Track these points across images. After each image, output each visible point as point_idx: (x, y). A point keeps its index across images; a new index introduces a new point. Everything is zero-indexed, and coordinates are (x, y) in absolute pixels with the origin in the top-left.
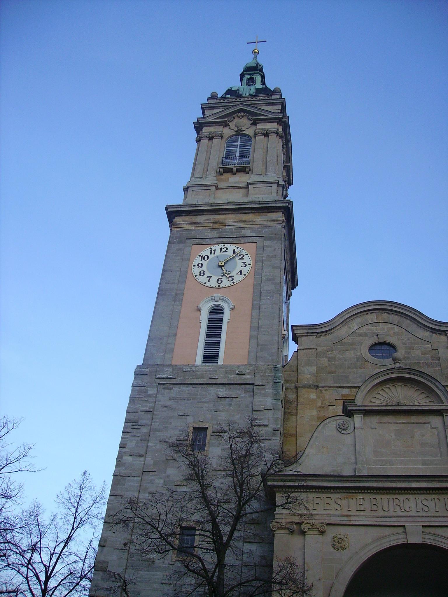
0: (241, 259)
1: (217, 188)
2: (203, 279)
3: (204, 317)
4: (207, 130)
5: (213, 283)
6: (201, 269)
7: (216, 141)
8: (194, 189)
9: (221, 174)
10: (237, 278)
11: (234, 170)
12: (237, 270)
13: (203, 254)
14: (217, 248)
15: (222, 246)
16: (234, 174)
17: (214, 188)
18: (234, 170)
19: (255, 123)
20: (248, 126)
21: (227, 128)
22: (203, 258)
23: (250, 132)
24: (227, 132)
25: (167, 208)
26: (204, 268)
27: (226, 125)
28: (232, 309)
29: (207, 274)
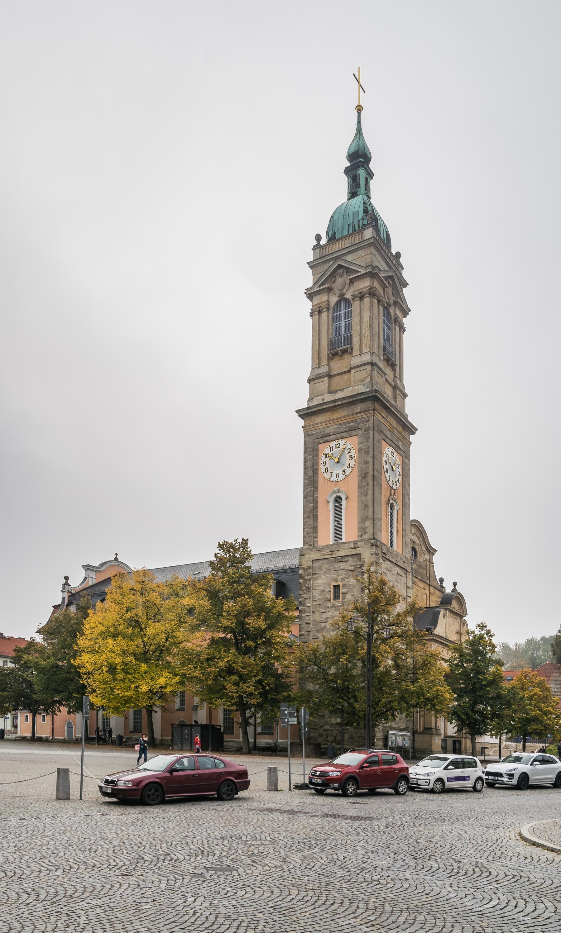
0: (349, 453)
1: (330, 376)
2: (327, 475)
3: (331, 506)
4: (317, 299)
5: (334, 479)
6: (325, 467)
7: (324, 315)
8: (315, 382)
9: (332, 359)
10: (348, 471)
11: (340, 353)
12: (347, 465)
13: (326, 453)
14: (333, 444)
15: (336, 442)
16: (341, 356)
17: (326, 379)
18: (340, 353)
19: (352, 281)
20: (347, 286)
21: (331, 294)
22: (326, 456)
23: (348, 296)
24: (334, 299)
25: (297, 411)
26: (327, 466)
27: (330, 290)
28: (347, 498)
29: (330, 471)
